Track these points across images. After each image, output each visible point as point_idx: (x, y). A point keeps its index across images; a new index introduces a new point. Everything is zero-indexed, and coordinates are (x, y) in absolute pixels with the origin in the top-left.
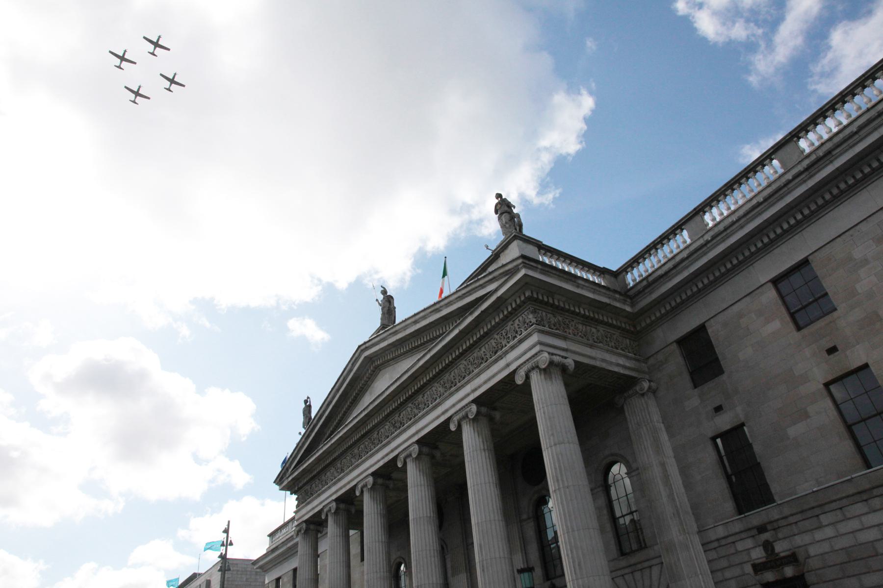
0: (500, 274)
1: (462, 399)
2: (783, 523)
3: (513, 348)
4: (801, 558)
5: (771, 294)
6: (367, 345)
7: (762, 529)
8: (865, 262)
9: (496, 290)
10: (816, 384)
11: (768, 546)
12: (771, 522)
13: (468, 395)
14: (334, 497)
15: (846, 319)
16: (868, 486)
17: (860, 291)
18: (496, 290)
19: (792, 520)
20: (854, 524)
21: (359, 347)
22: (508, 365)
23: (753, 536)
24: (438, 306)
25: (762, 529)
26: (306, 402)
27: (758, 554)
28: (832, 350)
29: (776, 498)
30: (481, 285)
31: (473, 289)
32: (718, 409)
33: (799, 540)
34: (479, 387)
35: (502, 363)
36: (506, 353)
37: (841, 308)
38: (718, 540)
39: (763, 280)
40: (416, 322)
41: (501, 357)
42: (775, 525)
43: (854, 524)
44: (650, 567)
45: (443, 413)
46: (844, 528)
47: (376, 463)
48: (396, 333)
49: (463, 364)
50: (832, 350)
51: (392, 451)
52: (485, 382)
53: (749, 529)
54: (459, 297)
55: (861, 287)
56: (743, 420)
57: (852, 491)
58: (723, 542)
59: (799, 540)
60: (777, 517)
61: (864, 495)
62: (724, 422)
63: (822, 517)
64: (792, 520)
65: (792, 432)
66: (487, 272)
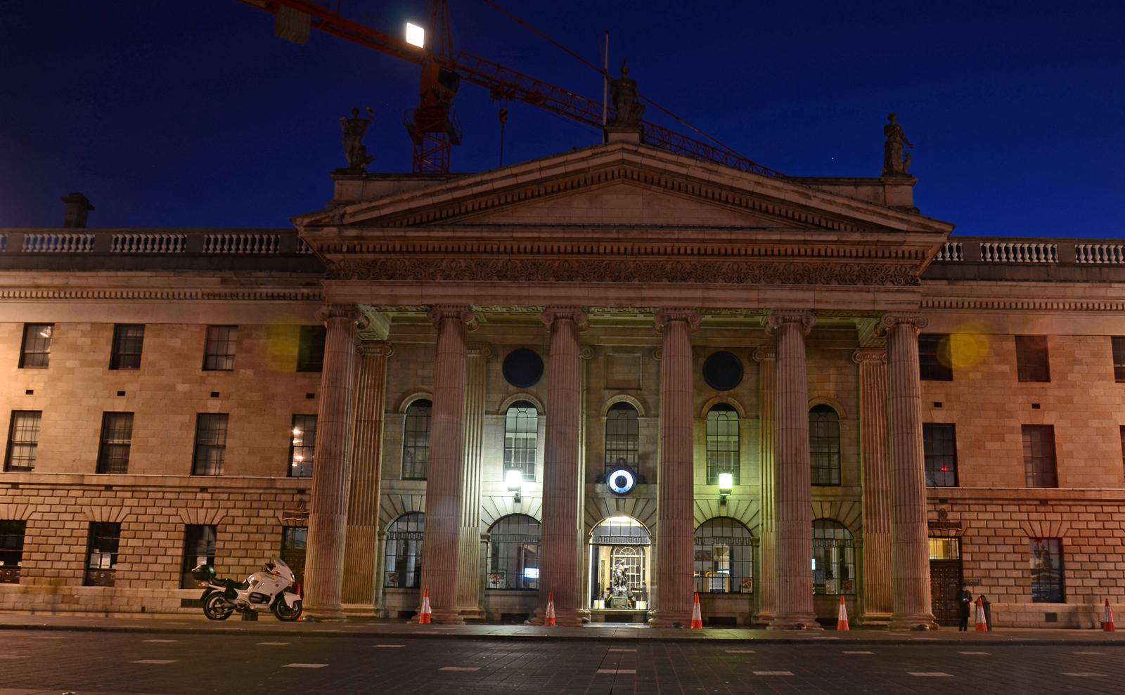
2: (960, 502)
4: (964, 527)
5: (1011, 345)
7: (943, 501)
8: (1080, 362)
10: (1017, 423)
11: (942, 513)
12: (952, 499)
15: (1052, 391)
16: (1025, 497)
17: (1069, 378)
19: (967, 502)
20: (1007, 516)
23: (934, 504)
25: (943, 501)
27: (935, 516)
28: (1036, 406)
29: (960, 484)
32: (938, 405)
33: (966, 515)
37: (1054, 382)
39: (1011, 332)
42: (954, 502)
43: (1007, 516)
46: (998, 516)
50: (1036, 406)
53: (934, 499)
55: (1071, 377)
56: (955, 420)
57: (1015, 497)
59: (966, 515)
60: (959, 496)
61: (1019, 501)
62: (939, 417)
63: (988, 507)
64: (967, 502)
65: (989, 445)
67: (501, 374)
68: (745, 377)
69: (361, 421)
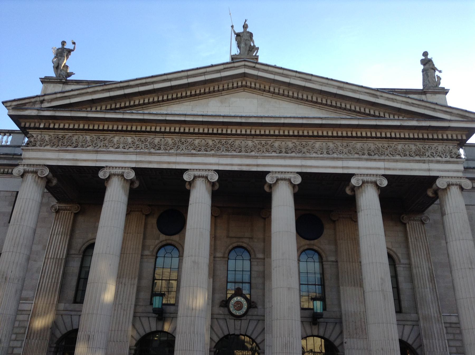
0: (458, 114)
1: (370, 168)
3: (438, 162)
9: (450, 121)
13: (379, 169)
14: (134, 165)
18: (450, 121)
24: (378, 93)
26: (63, 43)
30: (434, 109)
31: (426, 107)
34: (394, 169)
35: (425, 166)
36: (432, 162)
38: (450, 323)
40: (339, 88)
41: (424, 162)
44: (404, 325)
45: (343, 168)
47: (227, 165)
48: (254, 68)
49: (371, 145)
51: (258, 165)
52: (402, 169)
58: (453, 325)
66: (408, 96)
67: (155, 226)
68: (325, 232)
69: (48, 258)
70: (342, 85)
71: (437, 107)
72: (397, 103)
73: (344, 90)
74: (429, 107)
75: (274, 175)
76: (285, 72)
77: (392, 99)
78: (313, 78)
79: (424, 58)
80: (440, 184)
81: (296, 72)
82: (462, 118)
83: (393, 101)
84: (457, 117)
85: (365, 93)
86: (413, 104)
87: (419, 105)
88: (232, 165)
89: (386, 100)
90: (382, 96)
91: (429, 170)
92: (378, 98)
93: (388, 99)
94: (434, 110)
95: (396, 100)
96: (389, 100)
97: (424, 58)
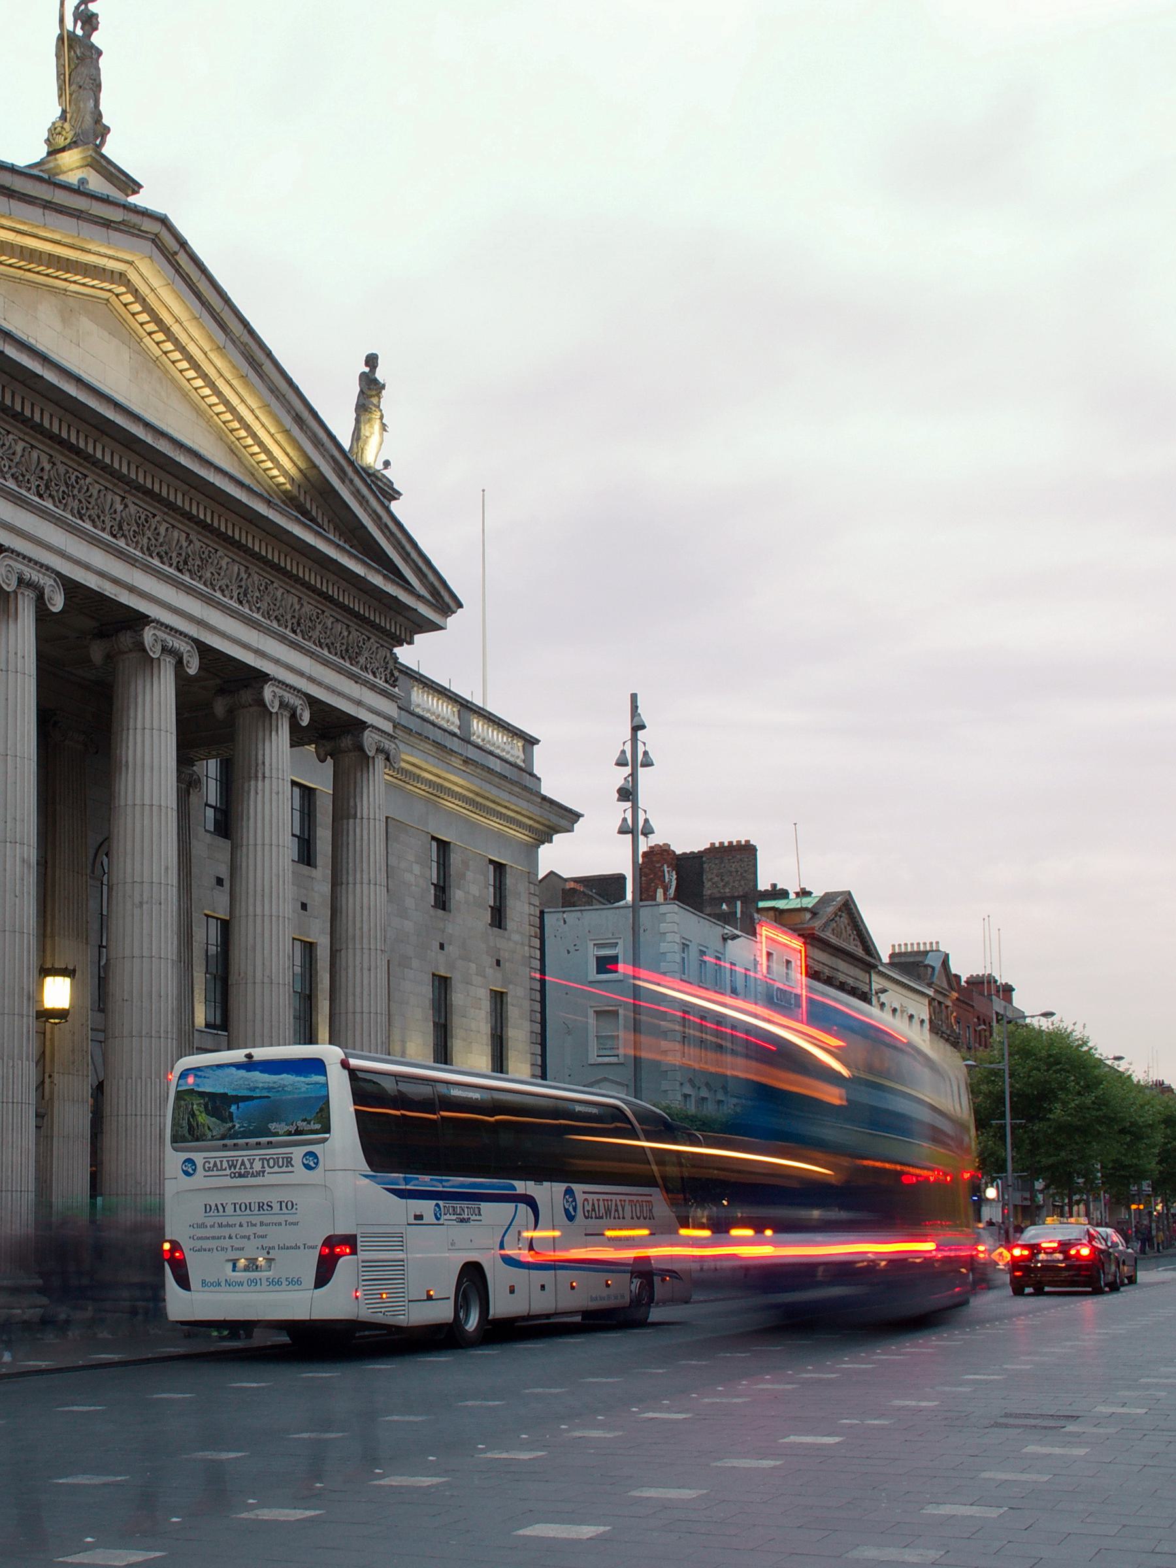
0: (432, 585)
6: (182, 259)
18: (419, 597)
21: (164, 221)
22: (359, 703)
24: (349, 470)
30: (408, 555)
31: (400, 543)
40: (299, 420)
51: (132, 589)
54: (380, 518)
70: (306, 415)
71: (414, 555)
72: (365, 510)
73: (301, 428)
74: (403, 548)
75: (159, 633)
76: (227, 315)
77: (363, 497)
78: (268, 367)
79: (367, 370)
80: (369, 740)
81: (251, 332)
82: (432, 595)
83: (361, 505)
84: (426, 588)
85: (332, 457)
86: (386, 526)
87: (392, 534)
88: (87, 567)
89: (352, 493)
90: (351, 481)
91: (359, 703)
92: (343, 482)
93: (357, 494)
94: (406, 557)
95: (367, 502)
96: (355, 497)
97: (367, 370)
